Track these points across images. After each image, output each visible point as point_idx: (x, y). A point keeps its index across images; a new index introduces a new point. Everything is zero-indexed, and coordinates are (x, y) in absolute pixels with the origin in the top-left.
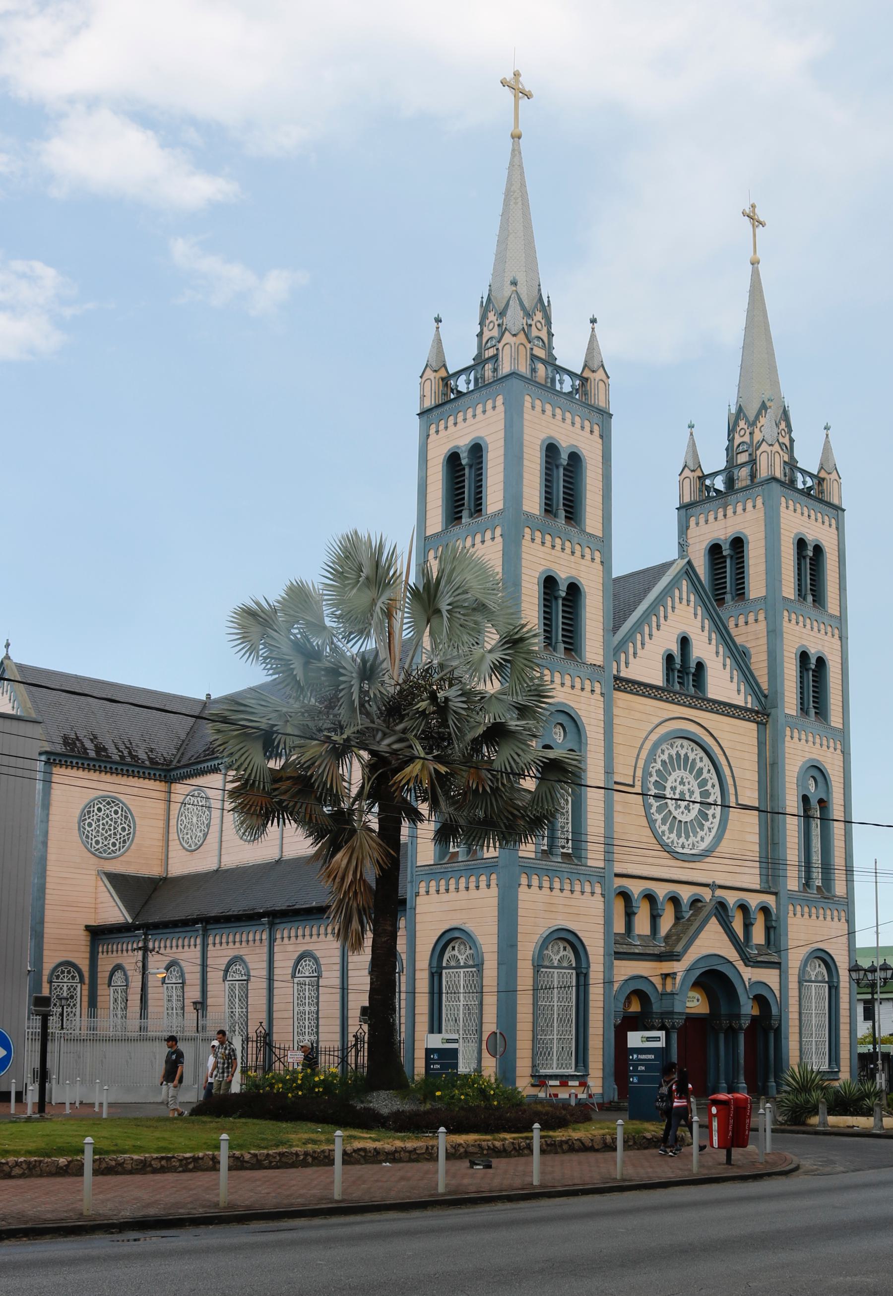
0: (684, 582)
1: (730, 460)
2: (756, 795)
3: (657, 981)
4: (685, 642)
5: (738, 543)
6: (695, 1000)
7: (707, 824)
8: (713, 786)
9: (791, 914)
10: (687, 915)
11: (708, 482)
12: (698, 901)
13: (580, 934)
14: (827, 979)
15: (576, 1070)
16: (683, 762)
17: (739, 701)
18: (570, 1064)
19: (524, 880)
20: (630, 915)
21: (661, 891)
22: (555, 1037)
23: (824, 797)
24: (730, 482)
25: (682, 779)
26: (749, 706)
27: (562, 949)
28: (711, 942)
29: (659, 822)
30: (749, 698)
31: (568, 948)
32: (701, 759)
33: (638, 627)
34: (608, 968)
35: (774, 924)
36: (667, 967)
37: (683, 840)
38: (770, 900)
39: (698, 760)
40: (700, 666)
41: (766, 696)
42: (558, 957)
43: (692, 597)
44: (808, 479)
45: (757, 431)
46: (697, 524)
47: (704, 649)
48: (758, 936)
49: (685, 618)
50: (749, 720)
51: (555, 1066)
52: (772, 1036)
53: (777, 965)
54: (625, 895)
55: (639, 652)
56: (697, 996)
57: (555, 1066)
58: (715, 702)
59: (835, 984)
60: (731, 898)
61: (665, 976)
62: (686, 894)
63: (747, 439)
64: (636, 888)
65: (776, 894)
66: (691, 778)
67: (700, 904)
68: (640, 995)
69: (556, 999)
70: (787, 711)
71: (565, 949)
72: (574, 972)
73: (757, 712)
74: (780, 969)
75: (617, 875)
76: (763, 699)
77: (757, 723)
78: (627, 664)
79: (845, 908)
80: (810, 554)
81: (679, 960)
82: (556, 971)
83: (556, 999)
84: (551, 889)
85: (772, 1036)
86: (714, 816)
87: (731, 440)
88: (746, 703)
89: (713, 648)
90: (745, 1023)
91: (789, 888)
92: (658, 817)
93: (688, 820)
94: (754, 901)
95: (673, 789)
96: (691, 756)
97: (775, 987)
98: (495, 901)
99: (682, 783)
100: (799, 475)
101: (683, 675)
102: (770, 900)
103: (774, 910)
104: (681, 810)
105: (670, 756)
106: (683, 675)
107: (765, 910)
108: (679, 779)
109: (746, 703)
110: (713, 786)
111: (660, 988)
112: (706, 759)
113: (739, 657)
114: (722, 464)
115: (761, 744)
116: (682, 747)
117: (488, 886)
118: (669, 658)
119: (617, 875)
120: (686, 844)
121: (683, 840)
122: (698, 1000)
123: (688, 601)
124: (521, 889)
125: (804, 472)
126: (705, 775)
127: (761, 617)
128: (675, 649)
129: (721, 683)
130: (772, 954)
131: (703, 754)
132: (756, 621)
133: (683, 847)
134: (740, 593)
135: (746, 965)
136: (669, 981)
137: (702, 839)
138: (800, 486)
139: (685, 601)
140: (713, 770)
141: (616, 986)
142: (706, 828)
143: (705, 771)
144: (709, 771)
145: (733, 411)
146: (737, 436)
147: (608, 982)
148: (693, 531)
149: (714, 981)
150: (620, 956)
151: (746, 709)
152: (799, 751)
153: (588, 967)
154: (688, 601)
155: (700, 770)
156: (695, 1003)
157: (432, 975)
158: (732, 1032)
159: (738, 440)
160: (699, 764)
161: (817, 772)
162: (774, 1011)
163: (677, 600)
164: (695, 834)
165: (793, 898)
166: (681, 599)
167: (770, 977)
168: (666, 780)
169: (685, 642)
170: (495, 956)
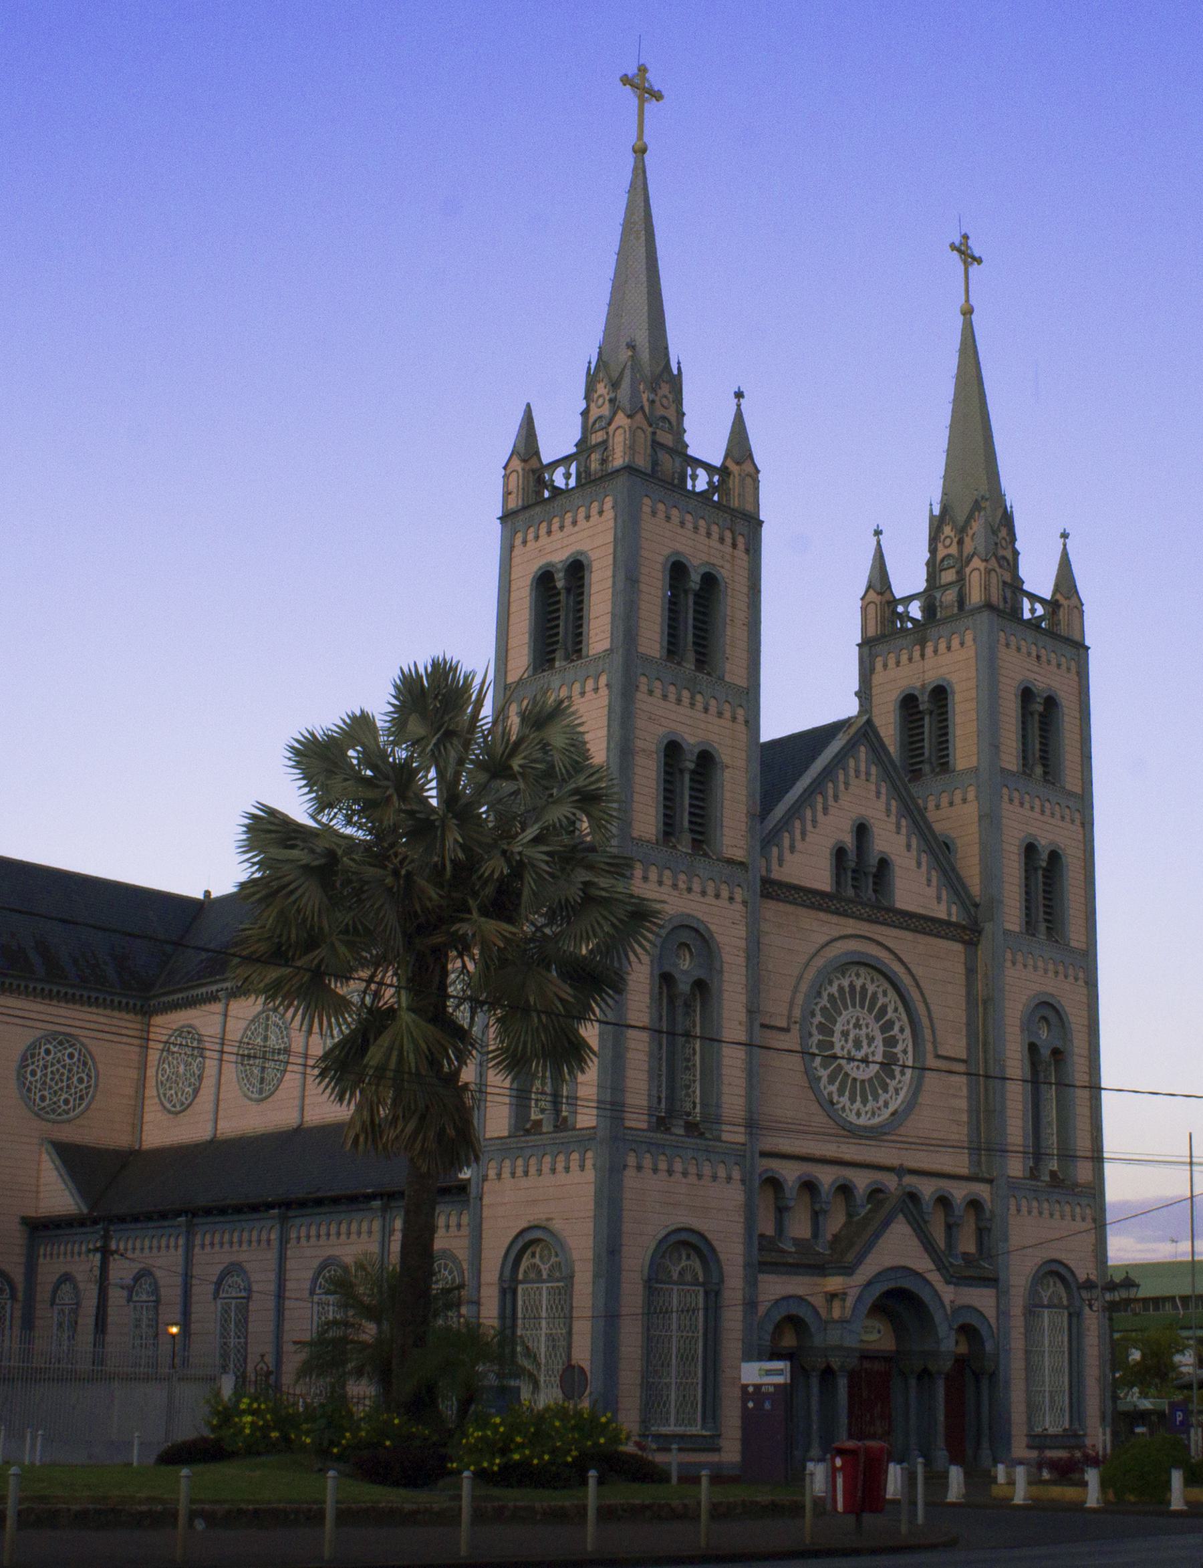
0: (863, 749)
1: (932, 577)
2: (963, 1042)
3: (819, 1302)
4: (862, 830)
5: (940, 693)
7: (892, 1084)
8: (902, 1030)
10: (863, 1212)
11: (900, 609)
12: (879, 1191)
13: (709, 1236)
14: (1065, 1303)
15: (703, 1427)
16: (857, 996)
17: (940, 912)
18: (695, 1420)
19: (631, 1160)
20: (781, 1211)
21: (826, 1177)
22: (673, 1380)
23: (1058, 1044)
24: (930, 609)
25: (858, 1019)
26: (954, 919)
27: (684, 1257)
28: (898, 1248)
29: (824, 1080)
30: (954, 909)
31: (693, 1255)
32: (885, 994)
33: (795, 811)
34: (751, 1283)
36: (834, 1283)
37: (858, 1104)
39: (880, 995)
40: (884, 864)
41: (976, 906)
43: (873, 770)
44: (1038, 606)
45: (967, 540)
46: (885, 666)
47: (890, 840)
49: (861, 800)
51: (672, 1420)
53: (991, 1281)
54: (774, 1183)
55: (799, 845)
56: (877, 1325)
57: (672, 1420)
60: (927, 1189)
61: (832, 1296)
62: (862, 1181)
63: (953, 550)
64: (790, 1173)
65: (990, 1181)
66: (870, 1019)
67: (881, 1196)
68: (794, 1322)
70: (1008, 926)
71: (688, 1257)
72: (701, 1290)
73: (964, 928)
75: (764, 1154)
76: (972, 910)
77: (964, 942)
78: (781, 862)
80: (1040, 708)
82: (675, 1288)
84: (670, 1172)
87: (933, 551)
88: (949, 914)
89: (902, 839)
92: (824, 1074)
93: (866, 1076)
94: (959, 1193)
95: (845, 1034)
96: (871, 989)
97: (990, 1313)
98: (591, 1189)
99: (857, 1026)
100: (1026, 600)
101: (860, 877)
102: (982, 1191)
103: (988, 1206)
105: (841, 988)
106: (860, 877)
107: (975, 1204)
108: (854, 1021)
109: (949, 914)
110: (902, 1030)
111: (823, 1312)
112: (892, 994)
113: (939, 852)
114: (920, 585)
115: (971, 971)
116: (858, 975)
117: (582, 1167)
118: (840, 853)
119: (764, 1154)
120: (863, 1110)
121: (858, 1104)
122: (879, 1332)
123: (868, 774)
125: (1033, 598)
126: (890, 1014)
127: (971, 795)
128: (849, 840)
129: (913, 888)
131: (887, 985)
132: (964, 801)
133: (858, 1114)
134: (944, 765)
135: (948, 1283)
136: (836, 1304)
137: (886, 1105)
138: (1027, 615)
139: (863, 776)
140: (901, 1009)
142: (891, 1089)
143: (890, 1010)
144: (896, 1010)
145: (937, 512)
146: (940, 546)
147: (751, 1305)
148: (878, 678)
149: (898, 1302)
150: (766, 1266)
151: (948, 924)
152: (1023, 982)
153: (722, 1281)
154: (868, 774)
155: (883, 1010)
156: (874, 1337)
157: (503, 1292)
159: (941, 554)
160: (881, 1001)
161: (1047, 1011)
162: (989, 1347)
163: (852, 773)
164: (876, 1099)
166: (857, 772)
167: (982, 1299)
168: (835, 1022)
169: (862, 830)
170: (590, 1266)
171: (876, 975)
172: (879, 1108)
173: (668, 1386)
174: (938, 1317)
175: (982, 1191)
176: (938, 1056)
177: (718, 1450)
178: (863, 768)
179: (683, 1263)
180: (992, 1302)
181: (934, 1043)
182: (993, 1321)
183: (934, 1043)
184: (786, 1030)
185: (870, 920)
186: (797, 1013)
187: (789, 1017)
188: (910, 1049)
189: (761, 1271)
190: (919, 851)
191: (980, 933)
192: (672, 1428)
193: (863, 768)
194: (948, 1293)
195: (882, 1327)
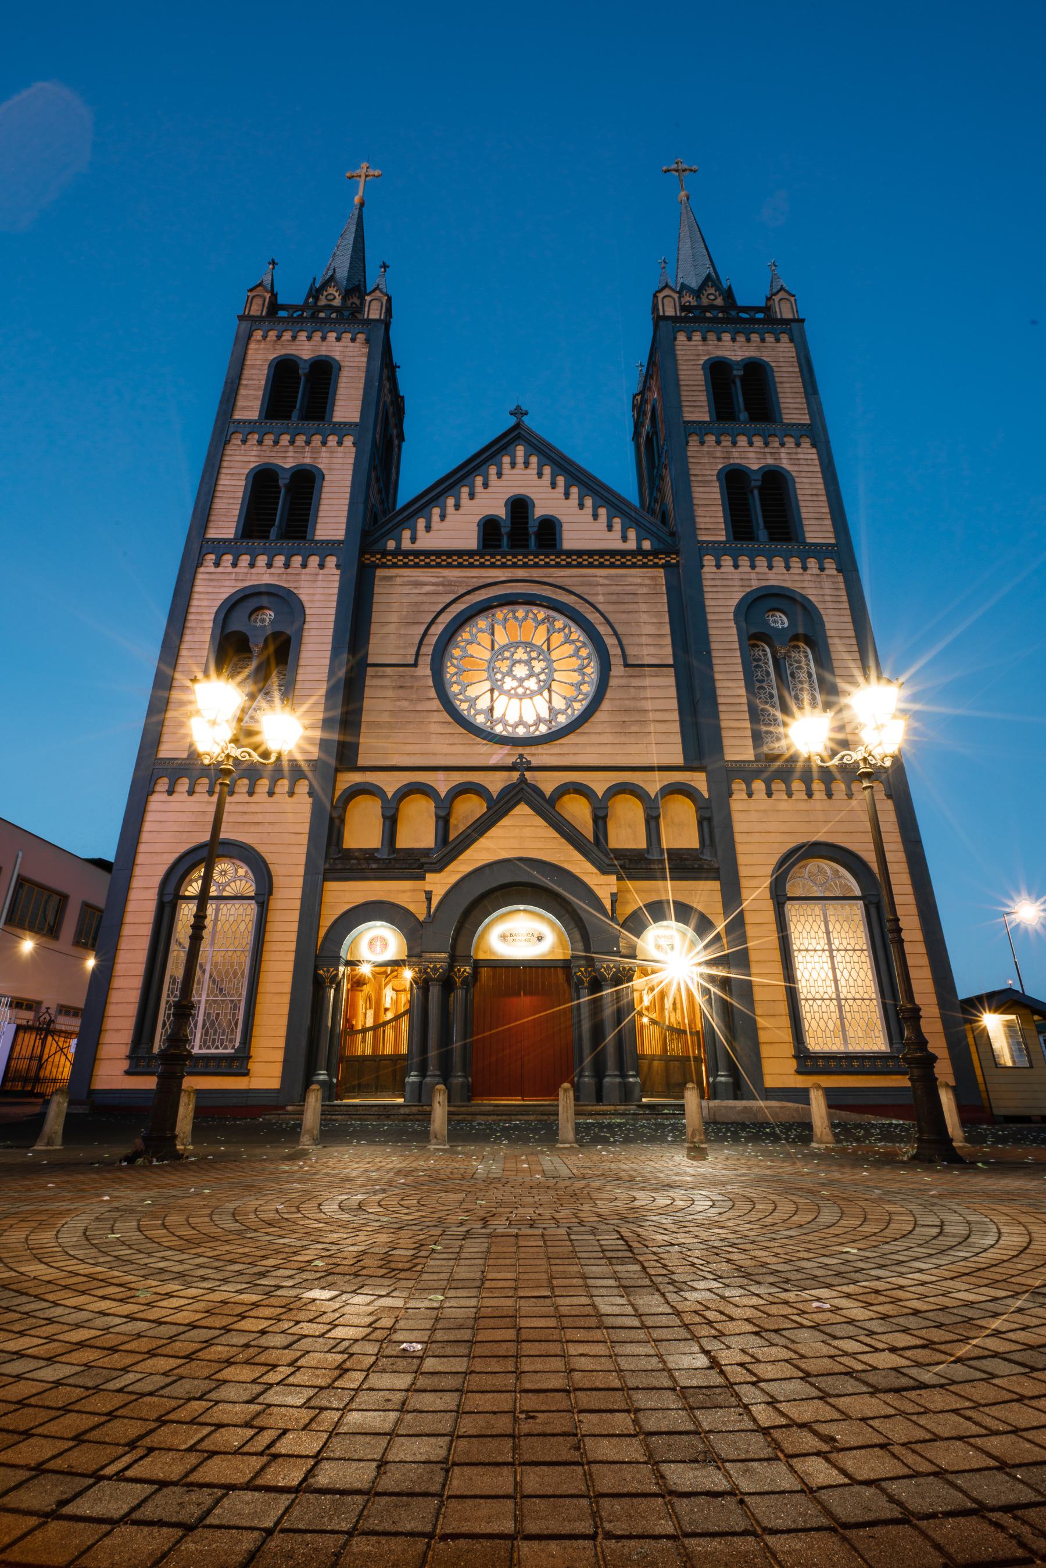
4: (519, 506)
18: (231, 1041)
38: (699, 781)
53: (712, 873)
58: (570, 553)
76: (669, 540)
77: (662, 566)
81: (439, 870)
123: (527, 464)
124: (154, 798)
128: (500, 511)
154: (527, 464)
166: (513, 465)
176: (626, 665)
177: (246, 1074)
178: (520, 460)
181: (624, 656)
183: (624, 656)
185: (525, 566)
193: (520, 460)
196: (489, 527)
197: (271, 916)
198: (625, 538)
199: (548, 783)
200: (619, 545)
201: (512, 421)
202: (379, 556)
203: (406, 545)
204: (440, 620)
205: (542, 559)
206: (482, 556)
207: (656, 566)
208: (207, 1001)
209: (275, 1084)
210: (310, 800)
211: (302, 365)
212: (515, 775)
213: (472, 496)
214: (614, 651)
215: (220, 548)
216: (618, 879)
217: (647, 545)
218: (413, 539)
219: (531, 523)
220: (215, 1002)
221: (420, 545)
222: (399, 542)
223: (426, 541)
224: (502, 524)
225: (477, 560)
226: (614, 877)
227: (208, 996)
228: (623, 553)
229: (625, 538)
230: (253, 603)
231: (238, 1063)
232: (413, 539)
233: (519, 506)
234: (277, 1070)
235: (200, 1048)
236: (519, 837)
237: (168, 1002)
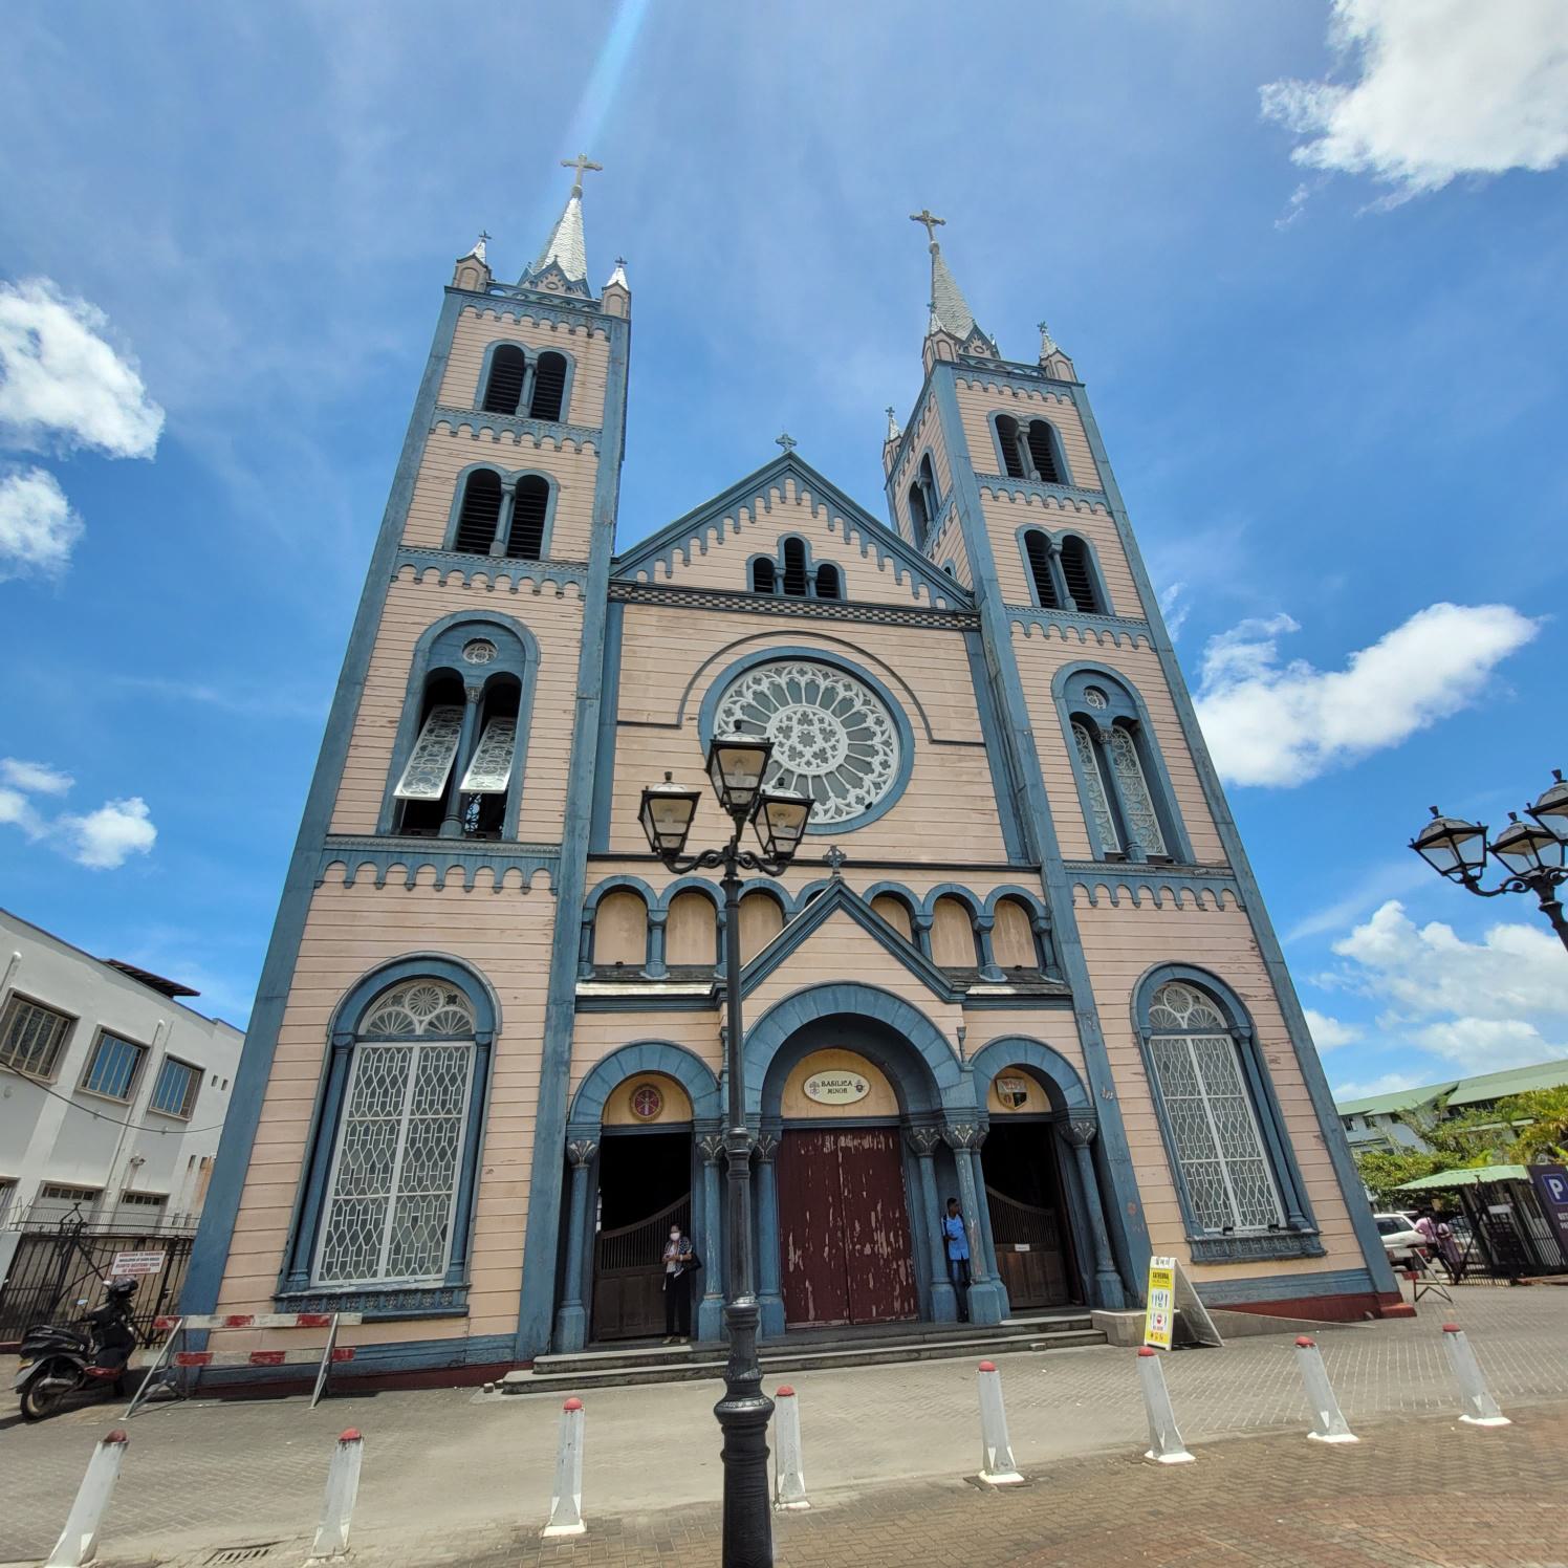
2: (978, 726)
4: (794, 548)
6: (852, 1089)
9: (1082, 901)
13: (477, 967)
14: (1224, 1025)
18: (435, 1260)
22: (393, 1194)
23: (1128, 713)
35: (1043, 924)
42: (427, 1018)
48: (1014, 947)
50: (942, 628)
52: (1085, 1156)
53: (1064, 1000)
56: (855, 1078)
58: (858, 606)
59: (1246, 1033)
65: (1038, 870)
69: (407, 1107)
73: (954, 614)
74: (1073, 1009)
76: (967, 600)
77: (961, 630)
79: (1231, 885)
82: (417, 1046)
83: (407, 1107)
85: (1085, 1156)
86: (885, 765)
90: (964, 1132)
91: (1065, 857)
93: (822, 772)
94: (981, 888)
102: (1027, 884)
104: (804, 760)
107: (1015, 900)
122: (860, 1088)
128: (775, 554)
130: (1049, 982)
141: (580, 1070)
147: (556, 1062)
151: (932, 611)
155: (847, 703)
156: (853, 1095)
158: (945, 1154)
162: (1072, 1097)
165: (1076, 872)
166: (783, 499)
171: (830, 670)
172: (848, 805)
173: (380, 1205)
174: (932, 1055)
175: (1027, 884)
176: (934, 742)
178: (791, 493)
179: (439, 1010)
180: (1072, 1030)
181: (928, 729)
182: (1076, 1061)
183: (928, 729)
184: (677, 727)
185: (806, 616)
186: (693, 708)
187: (681, 713)
188: (895, 741)
189: (577, 1011)
190: (881, 557)
191: (978, 616)
192: (381, 1278)
193: (791, 493)
194: (949, 1018)
195: (864, 1082)
196: (761, 569)
197: (499, 1065)
198: (916, 595)
199: (860, 883)
200: (911, 602)
201: (780, 452)
202: (629, 589)
203: (660, 578)
204: (706, 671)
205: (825, 610)
206: (755, 599)
207: (954, 629)
208: (399, 1198)
209: (509, 1327)
210: (554, 899)
211: (527, 354)
212: (826, 874)
213: (737, 530)
214: (915, 721)
215: (420, 561)
216: (964, 1009)
217: (941, 604)
218: (669, 573)
219: (808, 567)
220: (411, 1198)
221: (676, 581)
222: (650, 574)
223: (682, 577)
224: (776, 565)
225: (749, 604)
226: (960, 1006)
227: (400, 1190)
228: (919, 611)
229: (916, 595)
230: (482, 632)
231: (451, 1301)
232: (669, 573)
233: (794, 548)
234: (512, 1304)
235: (388, 1274)
236: (843, 956)
237: (336, 1201)
